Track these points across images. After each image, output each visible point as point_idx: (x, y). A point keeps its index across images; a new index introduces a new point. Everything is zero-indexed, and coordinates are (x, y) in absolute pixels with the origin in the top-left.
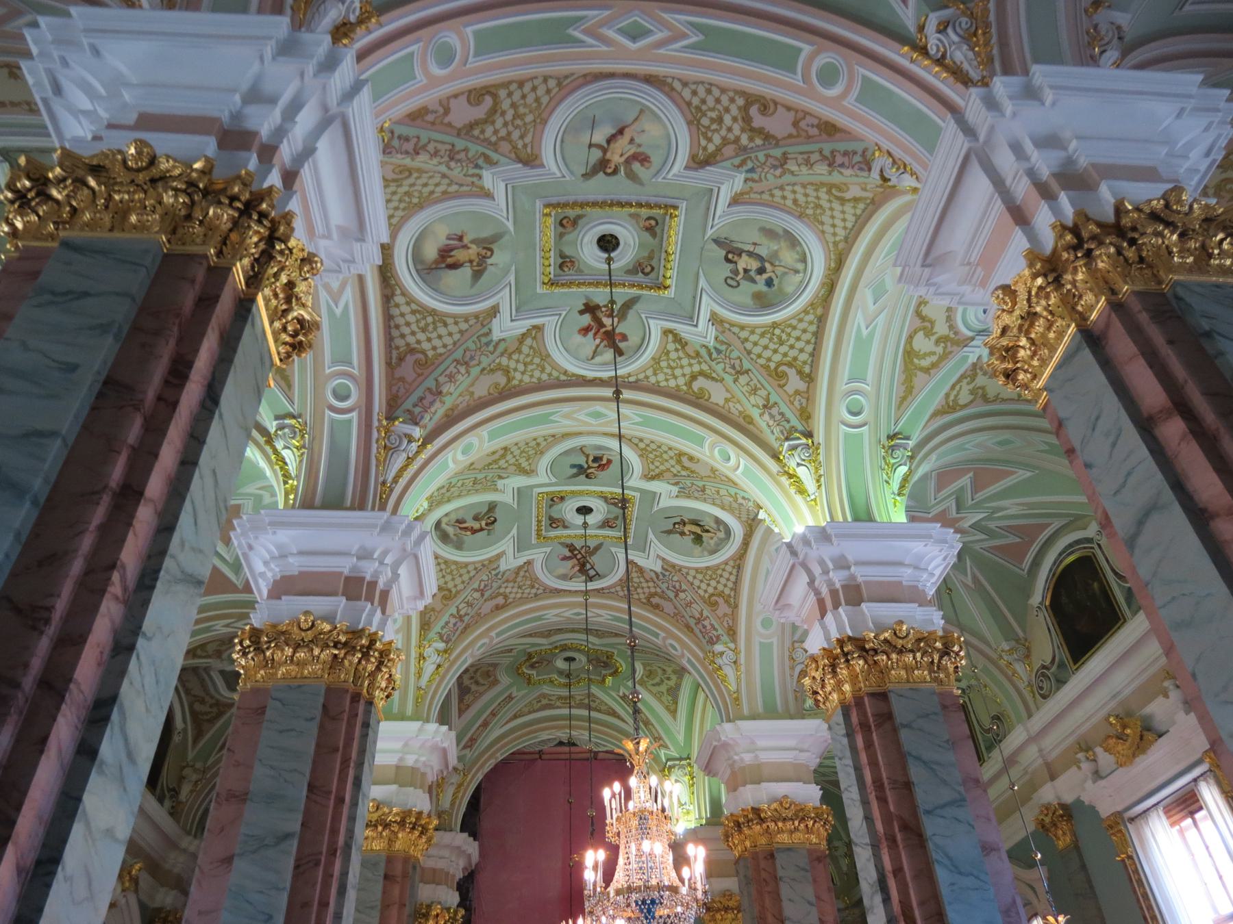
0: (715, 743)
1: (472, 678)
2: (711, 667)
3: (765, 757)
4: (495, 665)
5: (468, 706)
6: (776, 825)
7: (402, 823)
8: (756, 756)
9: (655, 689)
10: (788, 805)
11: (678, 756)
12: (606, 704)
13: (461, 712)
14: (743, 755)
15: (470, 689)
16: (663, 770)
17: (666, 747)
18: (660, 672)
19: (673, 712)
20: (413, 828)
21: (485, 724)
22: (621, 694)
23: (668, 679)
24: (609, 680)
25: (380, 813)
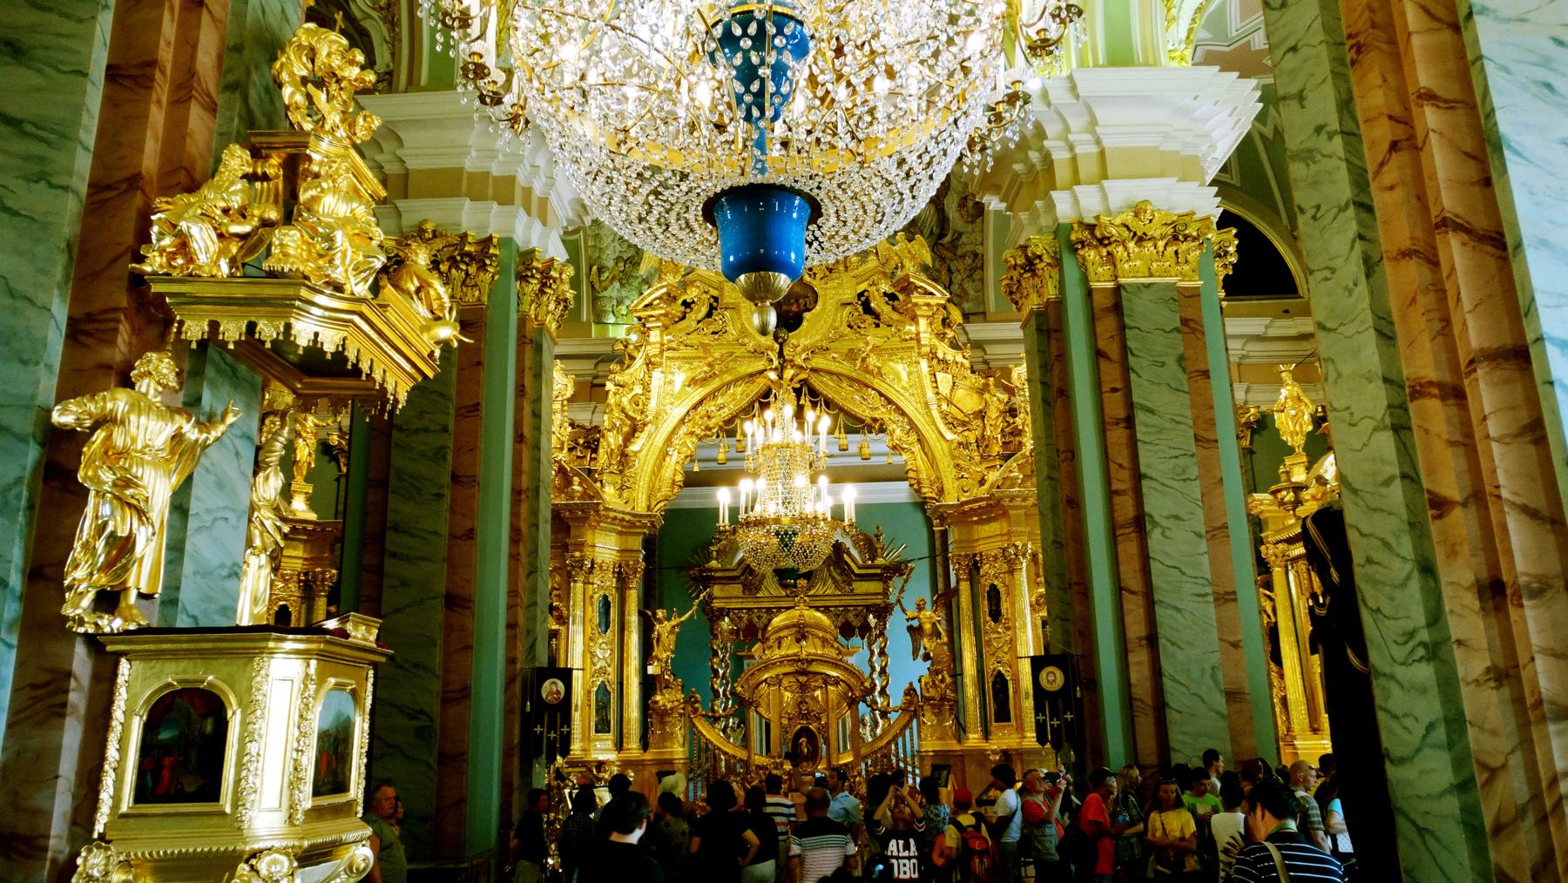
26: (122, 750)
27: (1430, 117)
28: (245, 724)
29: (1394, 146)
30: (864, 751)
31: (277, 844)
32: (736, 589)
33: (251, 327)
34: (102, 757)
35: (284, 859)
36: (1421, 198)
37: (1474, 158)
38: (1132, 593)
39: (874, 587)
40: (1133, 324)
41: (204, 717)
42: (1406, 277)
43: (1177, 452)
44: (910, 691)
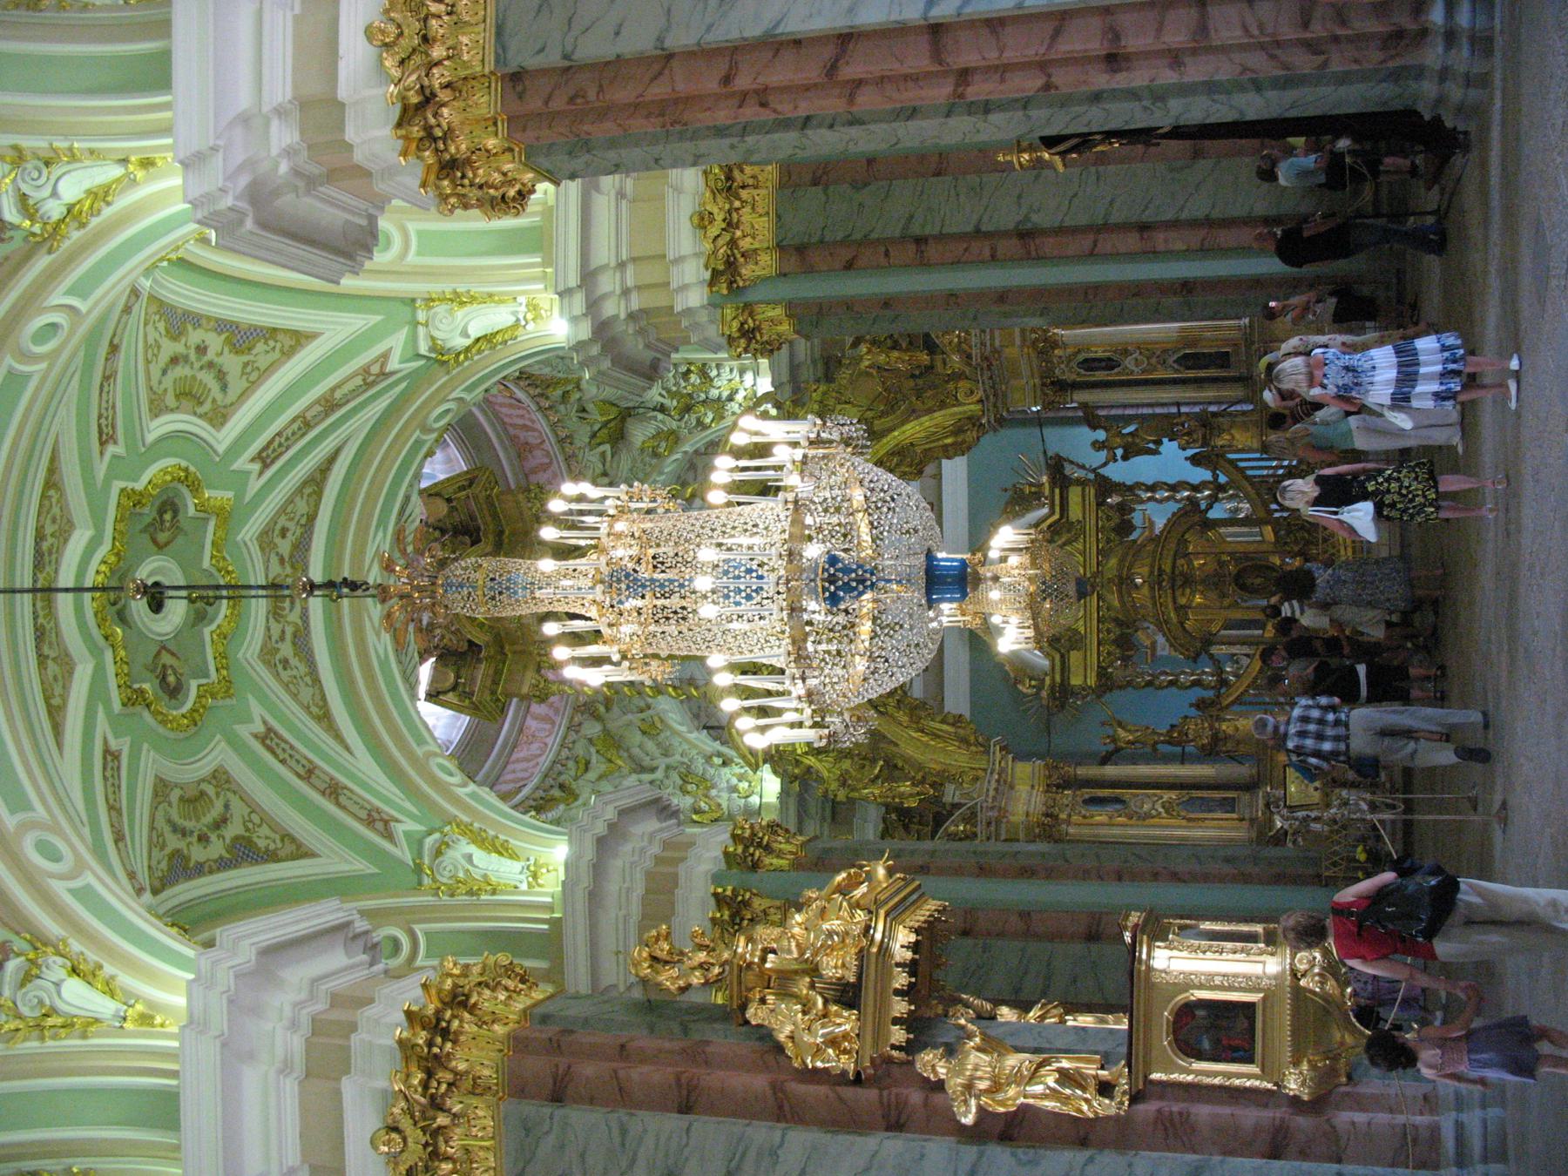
0: (249, 224)
1: (203, 839)
2: (76, 235)
3: (280, 89)
4: (162, 788)
5: (287, 837)
6: (438, 63)
7: (432, 1064)
8: (280, 112)
9: (236, 385)
10: (392, 29)
11: (405, 330)
12: (290, 501)
13: (301, 852)
14: (274, 152)
15: (236, 838)
16: (444, 363)
17: (385, 356)
18: (180, 371)
19: (300, 339)
20: (445, 1034)
21: (334, 791)
22: (257, 467)
23: (201, 350)
24: (217, 495)
25: (405, 1123)
26: (1215, 1074)
27: (743, 82)
28: (1201, 987)
29: (763, 105)
30: (1262, 514)
31: (1288, 961)
32: (1075, 657)
33: (897, 992)
34: (1221, 1087)
35: (1299, 955)
36: (807, 88)
37: (778, 50)
38: (1095, 243)
39: (1074, 494)
40: (819, 233)
41: (1194, 1016)
42: (867, 100)
43: (953, 192)
44: (1195, 460)
